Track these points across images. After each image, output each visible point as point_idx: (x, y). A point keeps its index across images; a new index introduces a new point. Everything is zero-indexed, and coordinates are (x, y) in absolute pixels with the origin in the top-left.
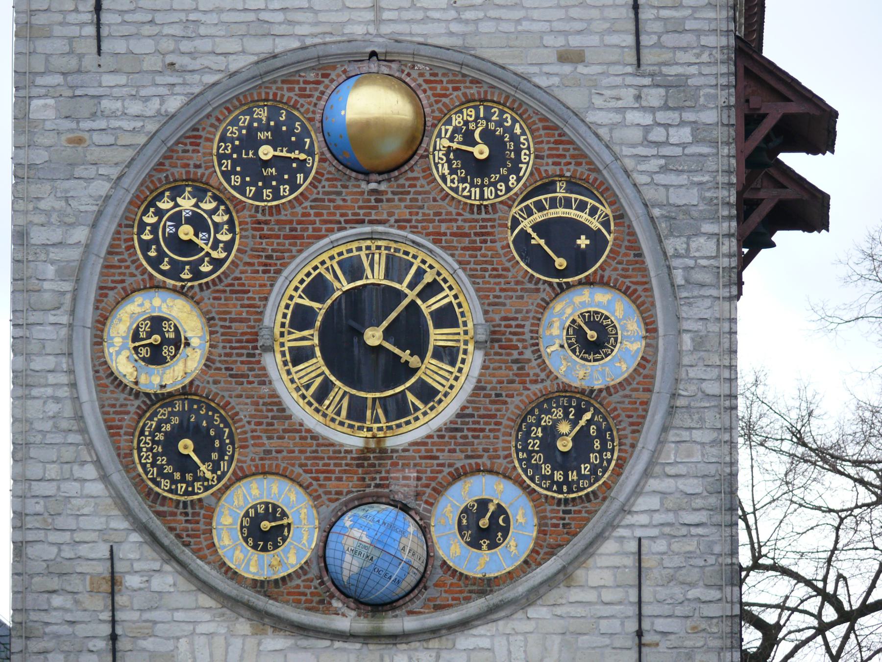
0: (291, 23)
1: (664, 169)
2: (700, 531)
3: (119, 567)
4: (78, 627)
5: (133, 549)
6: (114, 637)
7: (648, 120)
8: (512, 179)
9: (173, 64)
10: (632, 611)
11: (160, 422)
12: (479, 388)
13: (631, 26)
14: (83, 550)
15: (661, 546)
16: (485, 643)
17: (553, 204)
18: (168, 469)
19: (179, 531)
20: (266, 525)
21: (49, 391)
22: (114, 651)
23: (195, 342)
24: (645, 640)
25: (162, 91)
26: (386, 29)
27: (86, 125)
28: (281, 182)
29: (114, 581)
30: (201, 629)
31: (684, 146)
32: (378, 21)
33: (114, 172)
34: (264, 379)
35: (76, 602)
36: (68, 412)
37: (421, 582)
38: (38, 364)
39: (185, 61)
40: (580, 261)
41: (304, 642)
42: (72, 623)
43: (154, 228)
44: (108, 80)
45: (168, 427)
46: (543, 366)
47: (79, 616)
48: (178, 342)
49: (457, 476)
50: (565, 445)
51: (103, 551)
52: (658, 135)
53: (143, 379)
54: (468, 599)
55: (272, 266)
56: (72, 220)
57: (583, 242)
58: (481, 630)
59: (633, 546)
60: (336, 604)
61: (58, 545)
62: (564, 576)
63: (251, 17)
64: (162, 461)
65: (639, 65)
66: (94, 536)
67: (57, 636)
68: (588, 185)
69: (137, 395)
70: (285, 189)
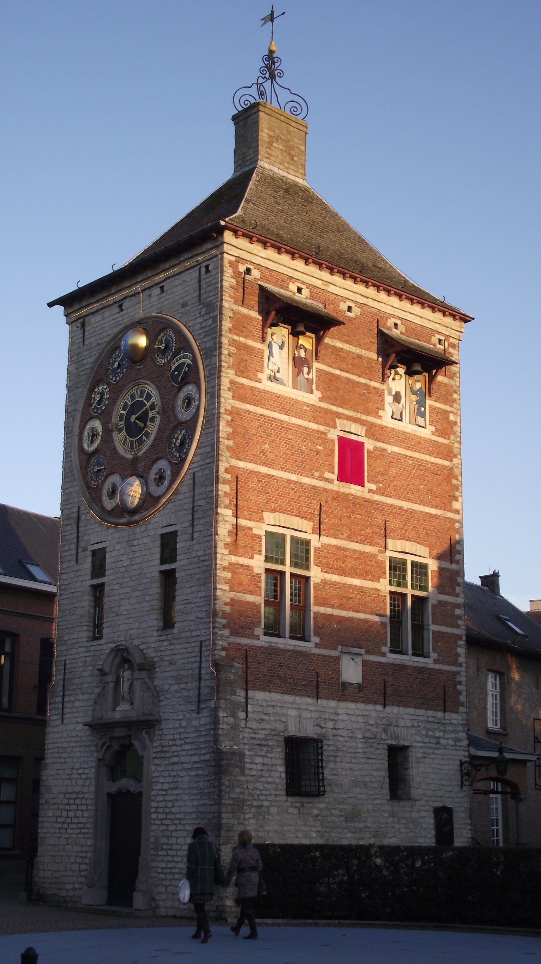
1: (205, 336)
3: (81, 513)
6: (78, 537)
15: (200, 474)
16: (157, 520)
24: (195, 509)
29: (79, 518)
30: (97, 530)
34: (113, 442)
44: (86, 353)
63: (115, 321)
65: (200, 301)
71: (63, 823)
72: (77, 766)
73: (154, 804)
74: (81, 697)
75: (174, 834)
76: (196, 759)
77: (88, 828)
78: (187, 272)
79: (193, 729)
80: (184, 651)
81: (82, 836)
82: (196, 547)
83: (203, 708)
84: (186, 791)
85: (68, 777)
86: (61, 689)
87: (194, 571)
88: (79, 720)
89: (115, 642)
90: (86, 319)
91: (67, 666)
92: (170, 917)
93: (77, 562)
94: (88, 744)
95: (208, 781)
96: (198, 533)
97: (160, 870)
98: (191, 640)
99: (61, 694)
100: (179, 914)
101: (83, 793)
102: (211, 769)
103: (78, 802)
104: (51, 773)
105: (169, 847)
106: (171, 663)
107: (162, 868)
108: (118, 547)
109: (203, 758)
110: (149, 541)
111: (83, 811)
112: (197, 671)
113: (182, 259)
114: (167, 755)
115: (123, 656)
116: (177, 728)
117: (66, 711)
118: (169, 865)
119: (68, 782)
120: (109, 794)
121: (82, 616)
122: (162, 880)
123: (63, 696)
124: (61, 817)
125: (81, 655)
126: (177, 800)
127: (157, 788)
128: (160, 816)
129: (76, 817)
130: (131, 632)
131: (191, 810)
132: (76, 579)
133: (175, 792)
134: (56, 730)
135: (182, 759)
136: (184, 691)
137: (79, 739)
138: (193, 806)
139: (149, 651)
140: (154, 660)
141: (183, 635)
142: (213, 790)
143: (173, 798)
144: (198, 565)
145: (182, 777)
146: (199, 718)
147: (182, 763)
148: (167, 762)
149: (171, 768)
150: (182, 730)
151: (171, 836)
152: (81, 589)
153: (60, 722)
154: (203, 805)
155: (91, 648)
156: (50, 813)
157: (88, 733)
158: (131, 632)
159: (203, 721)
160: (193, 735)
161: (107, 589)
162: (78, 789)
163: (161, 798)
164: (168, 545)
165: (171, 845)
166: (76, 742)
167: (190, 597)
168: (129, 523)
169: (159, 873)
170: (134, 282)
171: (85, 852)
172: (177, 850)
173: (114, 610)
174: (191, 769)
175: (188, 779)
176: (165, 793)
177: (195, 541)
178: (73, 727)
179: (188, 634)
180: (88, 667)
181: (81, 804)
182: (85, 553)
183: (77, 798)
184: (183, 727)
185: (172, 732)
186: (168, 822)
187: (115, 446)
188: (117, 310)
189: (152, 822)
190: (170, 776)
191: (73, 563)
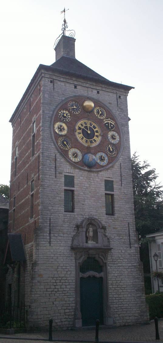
0: (77, 92)
1: (121, 119)
2: (127, 163)
3: (57, 158)
4: (51, 165)
5: (58, 155)
7: (119, 113)
8: (104, 117)
9: (63, 94)
10: (120, 172)
11: (61, 139)
12: (101, 141)
13: (117, 101)
14: (52, 155)
16: (103, 174)
17: (108, 120)
18: (62, 145)
19: (64, 154)
20: (75, 155)
21: (47, 132)
22: (56, 169)
23: (66, 129)
24: (122, 176)
25: (62, 97)
26: (89, 95)
27: (52, 99)
28: (76, 111)
30: (67, 167)
31: (123, 116)
32: (88, 94)
33: (56, 106)
34: (75, 136)
35: (50, 161)
36: (50, 136)
37: (95, 165)
38: (46, 129)
39: (65, 94)
40: (112, 128)
41: (80, 171)
42: (50, 164)
43: (61, 114)
44: (55, 94)
45: (62, 140)
46: (108, 140)
47: (51, 163)
48: (64, 129)
49: (99, 152)
50: (111, 150)
51: (54, 155)
52: (120, 115)
53: (59, 133)
54: (101, 168)
55: (76, 122)
56: (50, 110)
57: (112, 126)
58: (102, 172)
59: (120, 164)
60: (84, 166)
61: (48, 153)
62: (112, 167)
64: (62, 144)
66: (53, 153)
67: (48, 166)
68: (113, 119)
69: (59, 135)
70: (77, 112)
71: (52, 291)
72: (62, 265)
73: (109, 282)
74: (62, 235)
75: (122, 293)
76: (130, 265)
77: (70, 293)
78: (111, 93)
79: (128, 254)
80: (120, 225)
81: (66, 297)
82: (123, 189)
83: (132, 247)
84: (127, 277)
85: (56, 270)
86: (48, 230)
87: (123, 197)
88: (62, 245)
89: (82, 215)
90: (55, 81)
91: (51, 221)
92: (122, 326)
93: (56, 177)
94: (68, 256)
95: (137, 273)
96: (124, 185)
97: (115, 308)
98: (122, 221)
99: (48, 232)
100: (127, 324)
101: (66, 277)
102: (137, 269)
103: (62, 281)
104: (42, 268)
105: (120, 298)
106: (114, 228)
107: (116, 307)
108: (82, 178)
109: (133, 265)
110: (99, 180)
111: (66, 285)
112: (128, 233)
113: (110, 88)
114: (115, 263)
115: (92, 222)
116: (120, 253)
117: (51, 240)
118: (120, 306)
119: (56, 272)
120: (82, 279)
121: (60, 201)
122: (116, 312)
123: (50, 233)
124: (50, 288)
125: (61, 217)
126: (122, 280)
127: (111, 275)
128: (114, 286)
129: (61, 288)
130: (92, 213)
131: (130, 284)
132: (55, 184)
133: (121, 277)
134: (45, 248)
135: (124, 265)
136: (122, 239)
137: (62, 253)
138: (130, 282)
139: (103, 222)
140: (105, 226)
141: (120, 219)
142: (139, 276)
143: (120, 279)
144: (124, 195)
145: (124, 271)
146: (130, 250)
147: (124, 266)
148: (116, 265)
149: (118, 268)
150: (123, 254)
151: (120, 294)
152: (59, 189)
153: (49, 245)
154: (135, 282)
155: (67, 215)
156: (42, 287)
157: (68, 251)
158: (92, 213)
159: (132, 251)
160: (129, 256)
161: (75, 193)
162: (63, 275)
163: (114, 279)
164: (109, 185)
165: (121, 298)
166: (60, 254)
167: (121, 206)
168: (89, 171)
169: (114, 309)
170: (86, 82)
171: (68, 304)
172: (124, 299)
173: (81, 202)
174: (129, 268)
175: (127, 272)
176: (116, 277)
177: (122, 187)
178: (58, 247)
179: (122, 219)
180: (66, 223)
181: (65, 282)
182: (61, 175)
183: (62, 280)
184: (123, 253)
185: (117, 254)
186: (119, 289)
187: (76, 138)
188: (74, 87)
189: (110, 289)
190: (118, 271)
191: (54, 177)
